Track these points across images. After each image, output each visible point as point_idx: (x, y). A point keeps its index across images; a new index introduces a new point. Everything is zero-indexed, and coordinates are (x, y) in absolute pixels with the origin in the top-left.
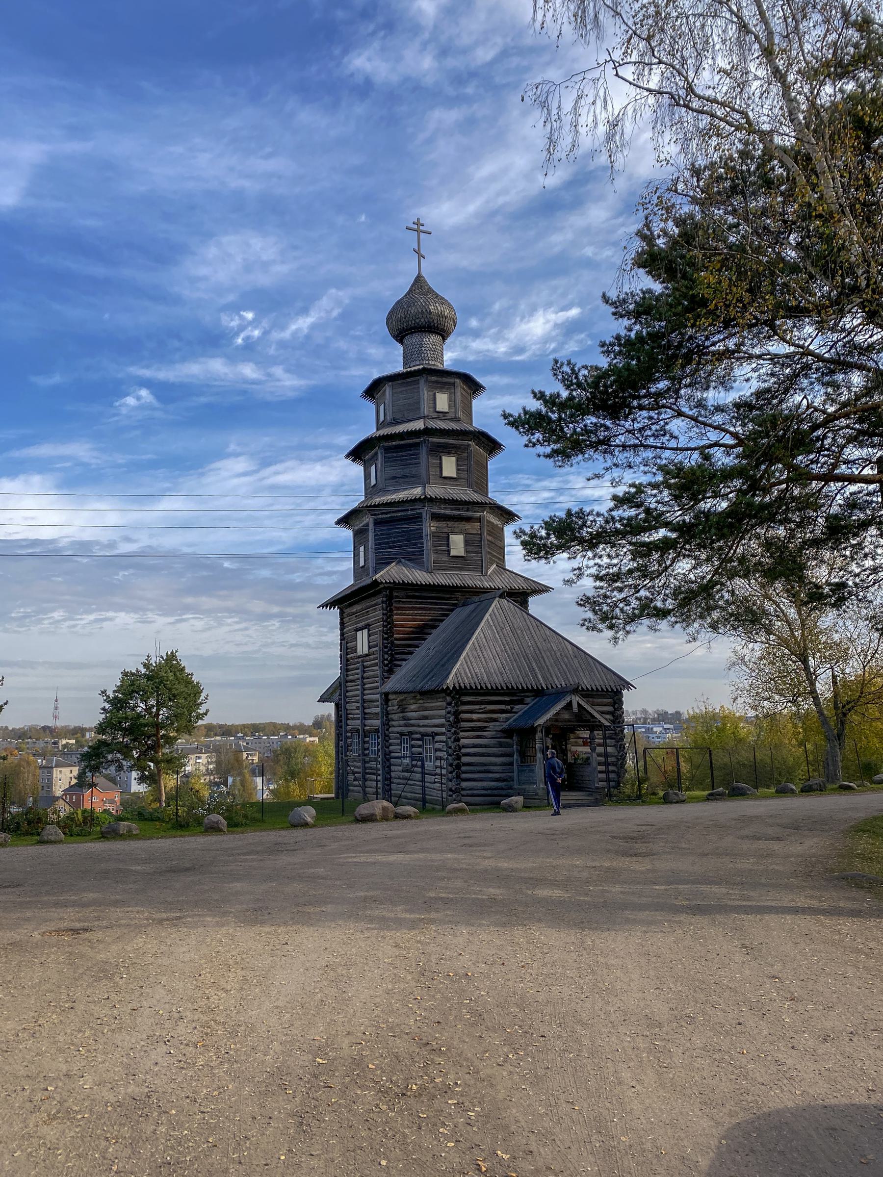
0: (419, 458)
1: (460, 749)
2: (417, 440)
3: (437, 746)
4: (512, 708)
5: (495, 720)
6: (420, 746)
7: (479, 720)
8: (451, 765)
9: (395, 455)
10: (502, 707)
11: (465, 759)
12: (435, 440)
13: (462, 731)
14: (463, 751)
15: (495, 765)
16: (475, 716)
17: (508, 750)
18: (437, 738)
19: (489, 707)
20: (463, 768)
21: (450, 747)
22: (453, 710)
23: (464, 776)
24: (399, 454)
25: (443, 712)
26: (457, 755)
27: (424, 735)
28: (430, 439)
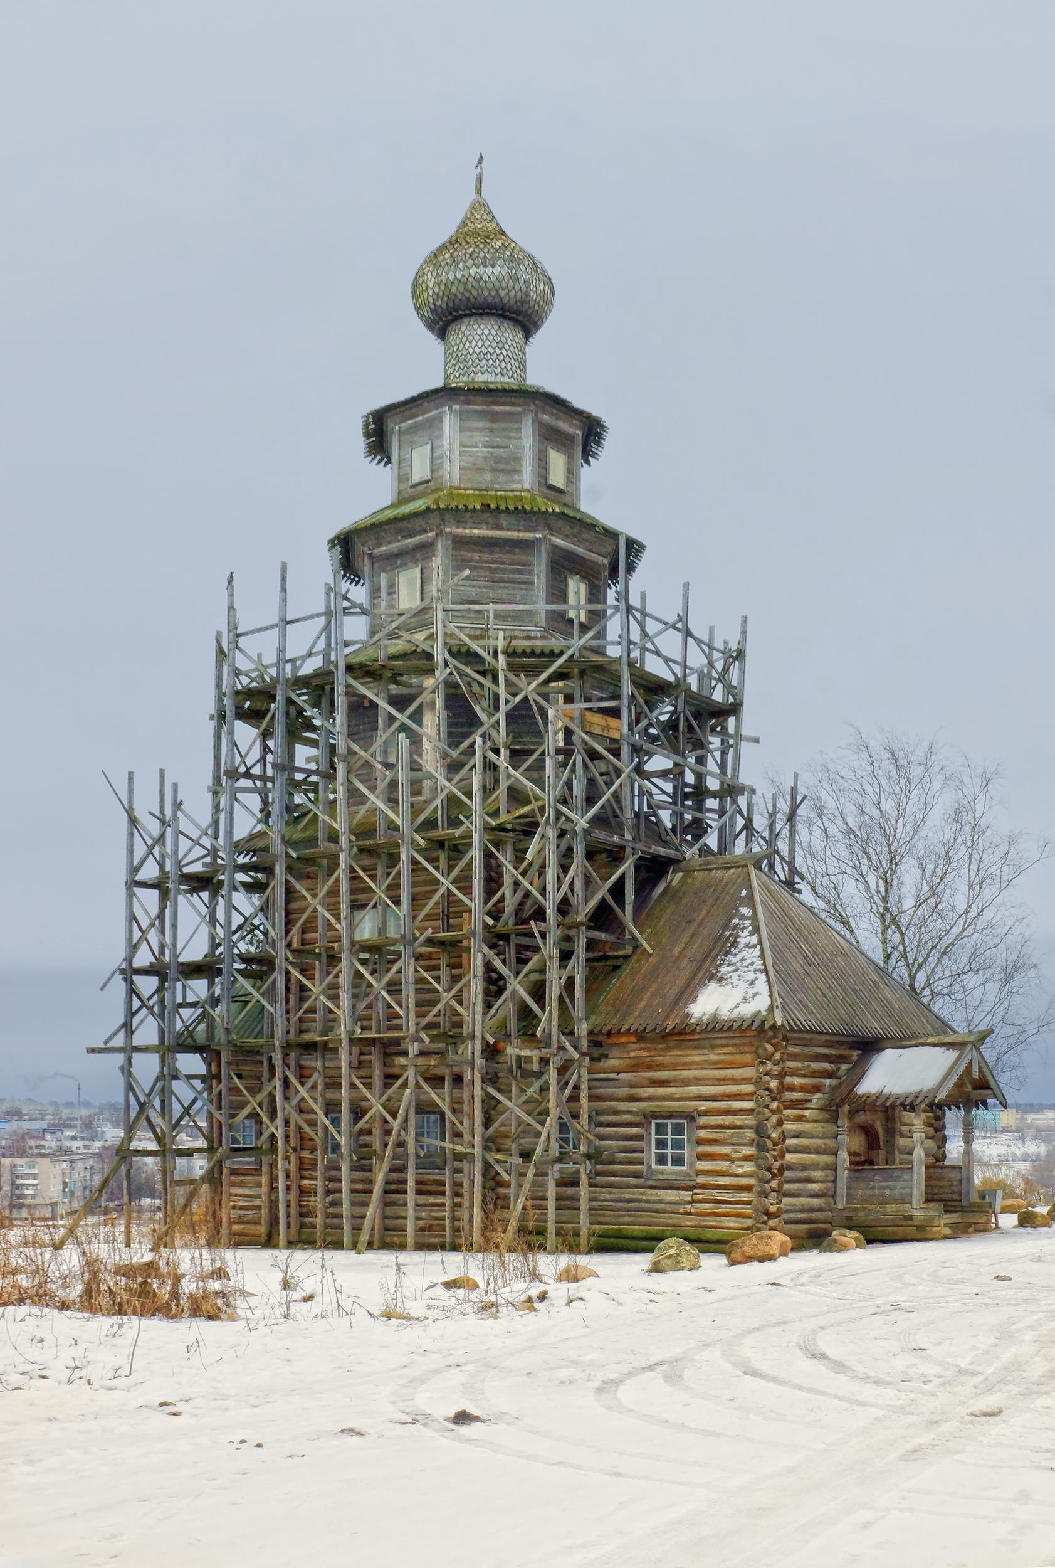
0: (531, 573)
1: (784, 1140)
2: (529, 536)
3: (702, 1134)
4: (838, 1069)
5: (817, 1089)
6: (639, 1137)
7: (802, 1089)
8: (769, 1169)
9: (476, 556)
10: (826, 1066)
11: (789, 1157)
12: (558, 540)
13: (786, 1108)
14: (791, 1142)
15: (816, 1167)
16: (797, 1081)
17: (831, 1143)
18: (703, 1120)
19: (815, 1066)
20: (787, 1174)
21: (769, 1137)
22: (776, 1069)
23: (786, 1186)
24: (487, 557)
25: (749, 1072)
26: (781, 1150)
27: (649, 1116)
28: (553, 539)
